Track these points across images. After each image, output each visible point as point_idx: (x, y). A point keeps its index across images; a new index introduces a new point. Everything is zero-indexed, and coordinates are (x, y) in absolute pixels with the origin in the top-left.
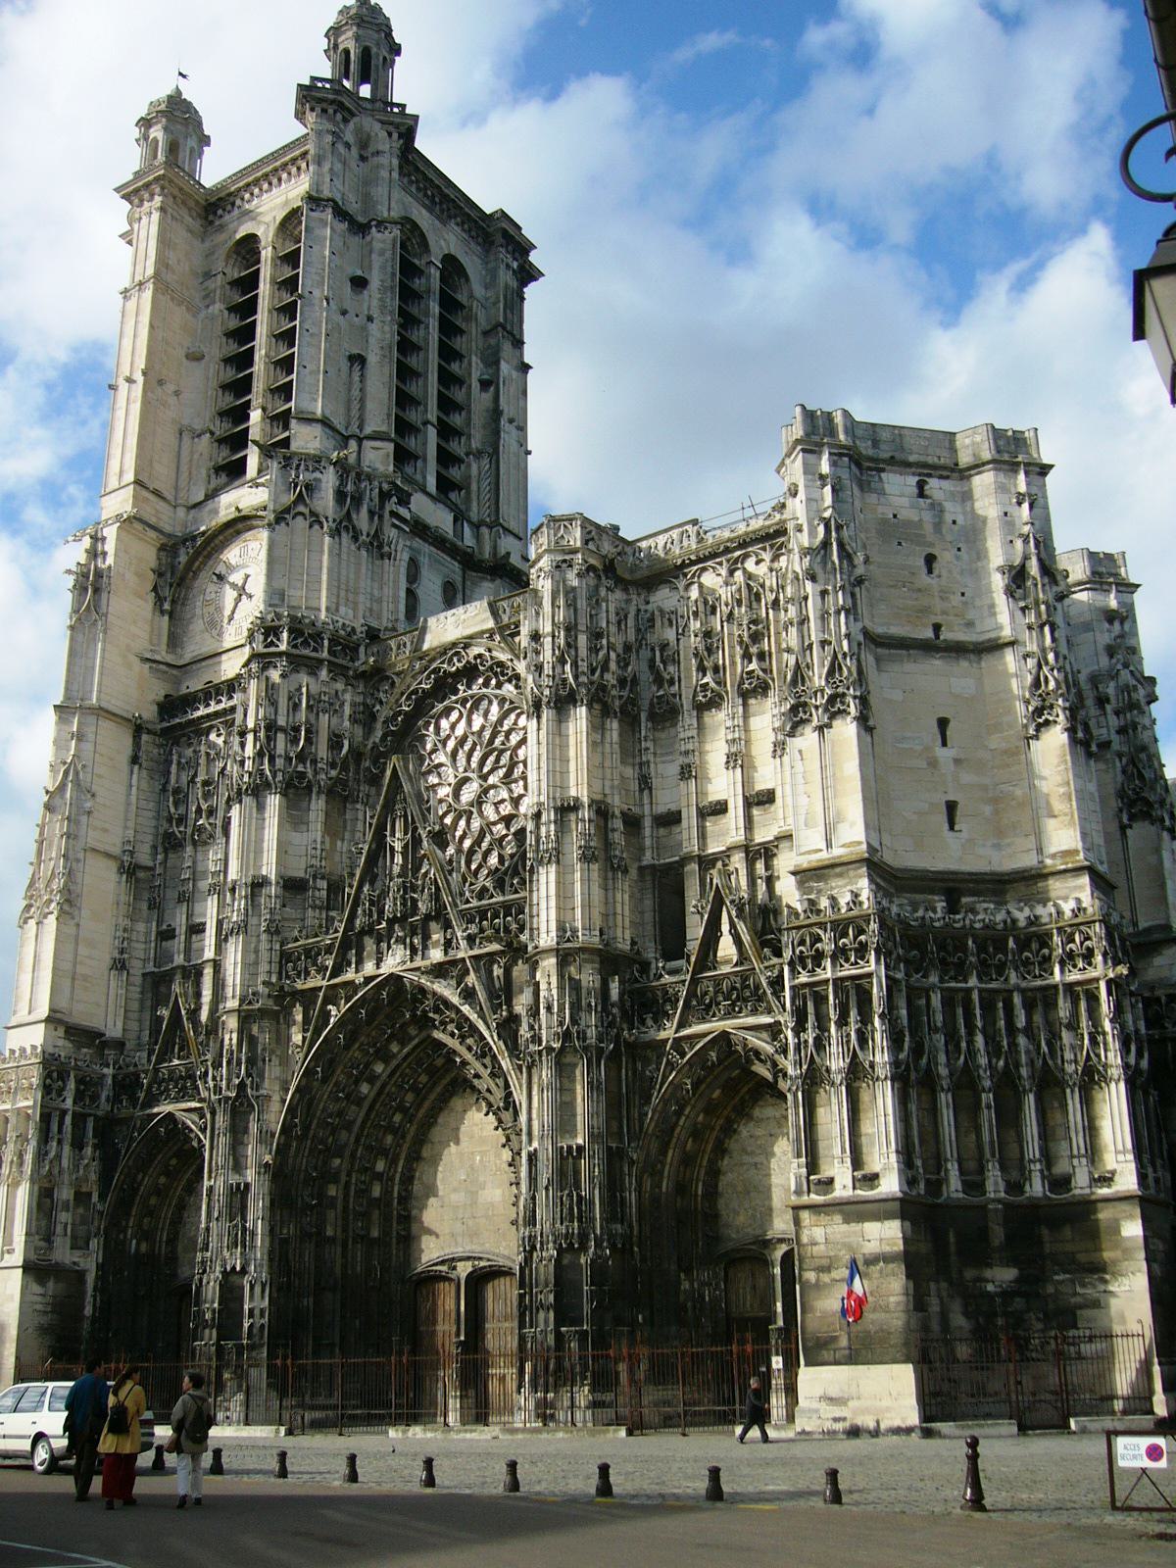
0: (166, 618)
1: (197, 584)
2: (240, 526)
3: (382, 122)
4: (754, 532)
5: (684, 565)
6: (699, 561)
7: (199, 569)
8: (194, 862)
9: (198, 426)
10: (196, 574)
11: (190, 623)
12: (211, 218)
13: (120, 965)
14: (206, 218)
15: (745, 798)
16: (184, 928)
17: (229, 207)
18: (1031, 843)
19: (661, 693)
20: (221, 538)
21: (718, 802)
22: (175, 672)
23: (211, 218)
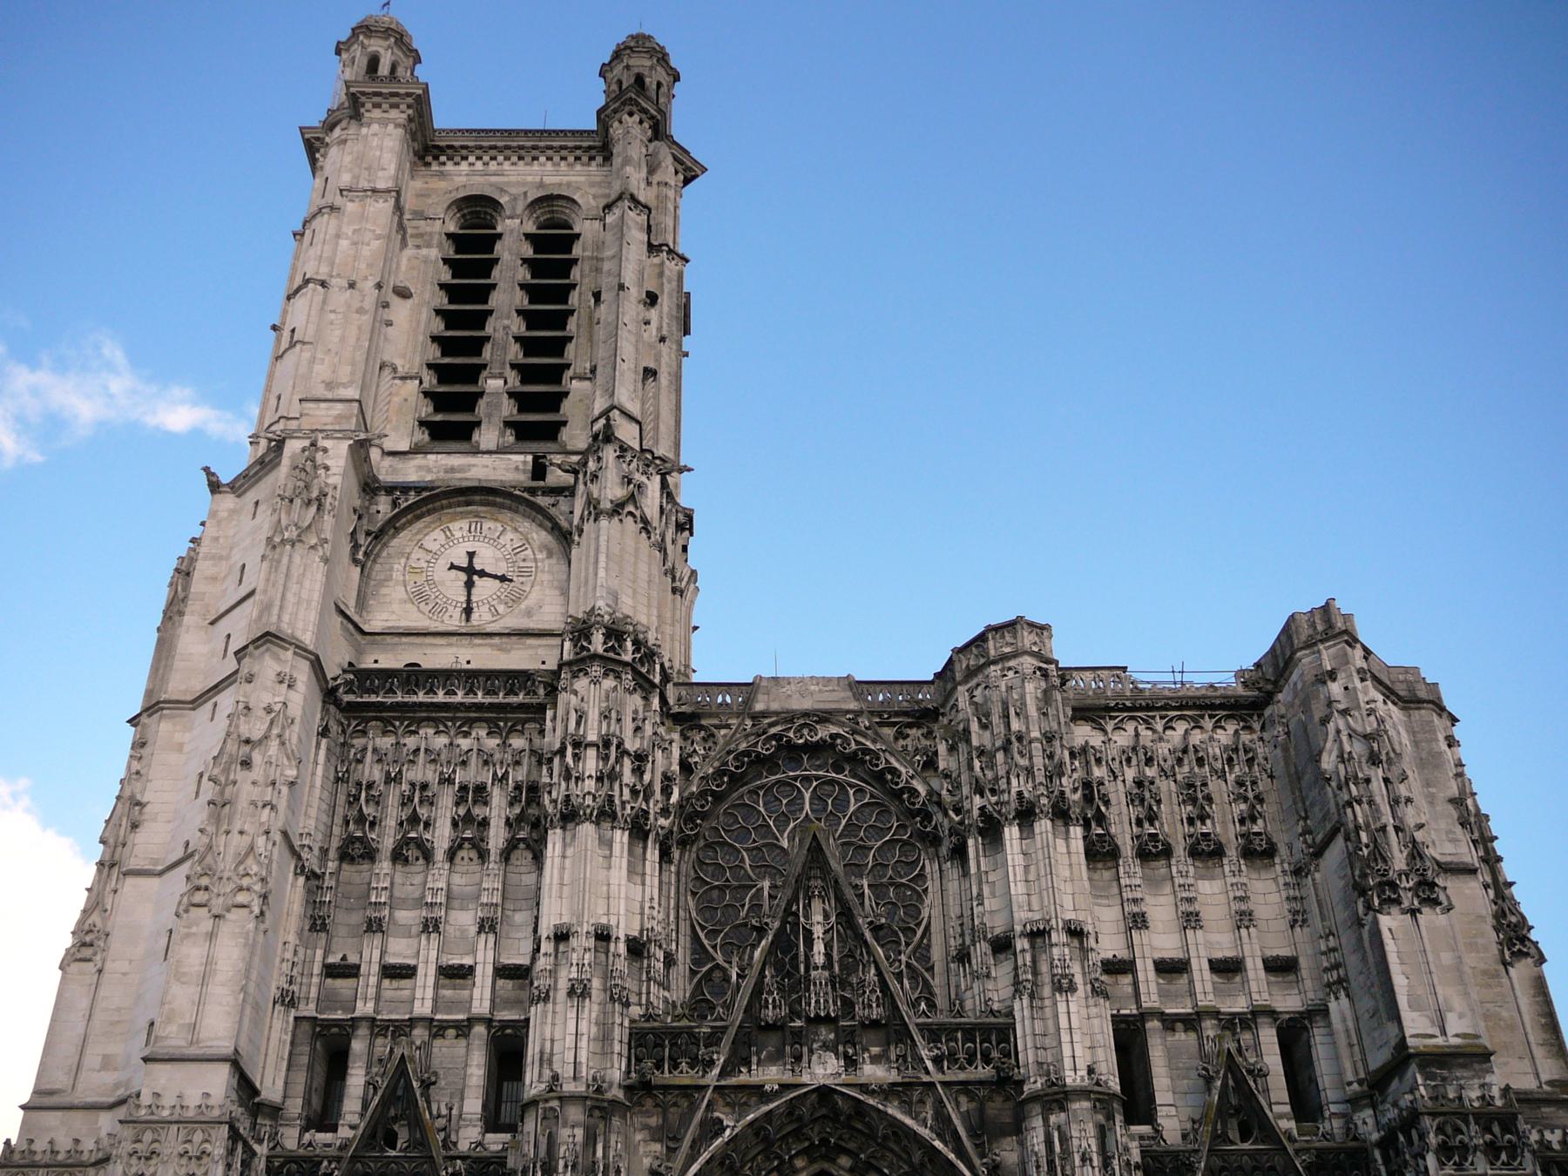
0: (359, 569)
1: (395, 542)
2: (477, 498)
3: (675, 158)
4: (1199, 698)
5: (1116, 708)
6: (1133, 709)
7: (403, 527)
8: (392, 884)
9: (403, 367)
10: (398, 530)
11: (381, 584)
12: (429, 159)
13: (287, 1000)
14: (422, 158)
15: (1210, 961)
16: (375, 968)
17: (457, 159)
18: (1526, 1065)
19: (1100, 831)
20: (444, 502)
21: (1180, 961)
22: (359, 637)
23: (429, 159)
